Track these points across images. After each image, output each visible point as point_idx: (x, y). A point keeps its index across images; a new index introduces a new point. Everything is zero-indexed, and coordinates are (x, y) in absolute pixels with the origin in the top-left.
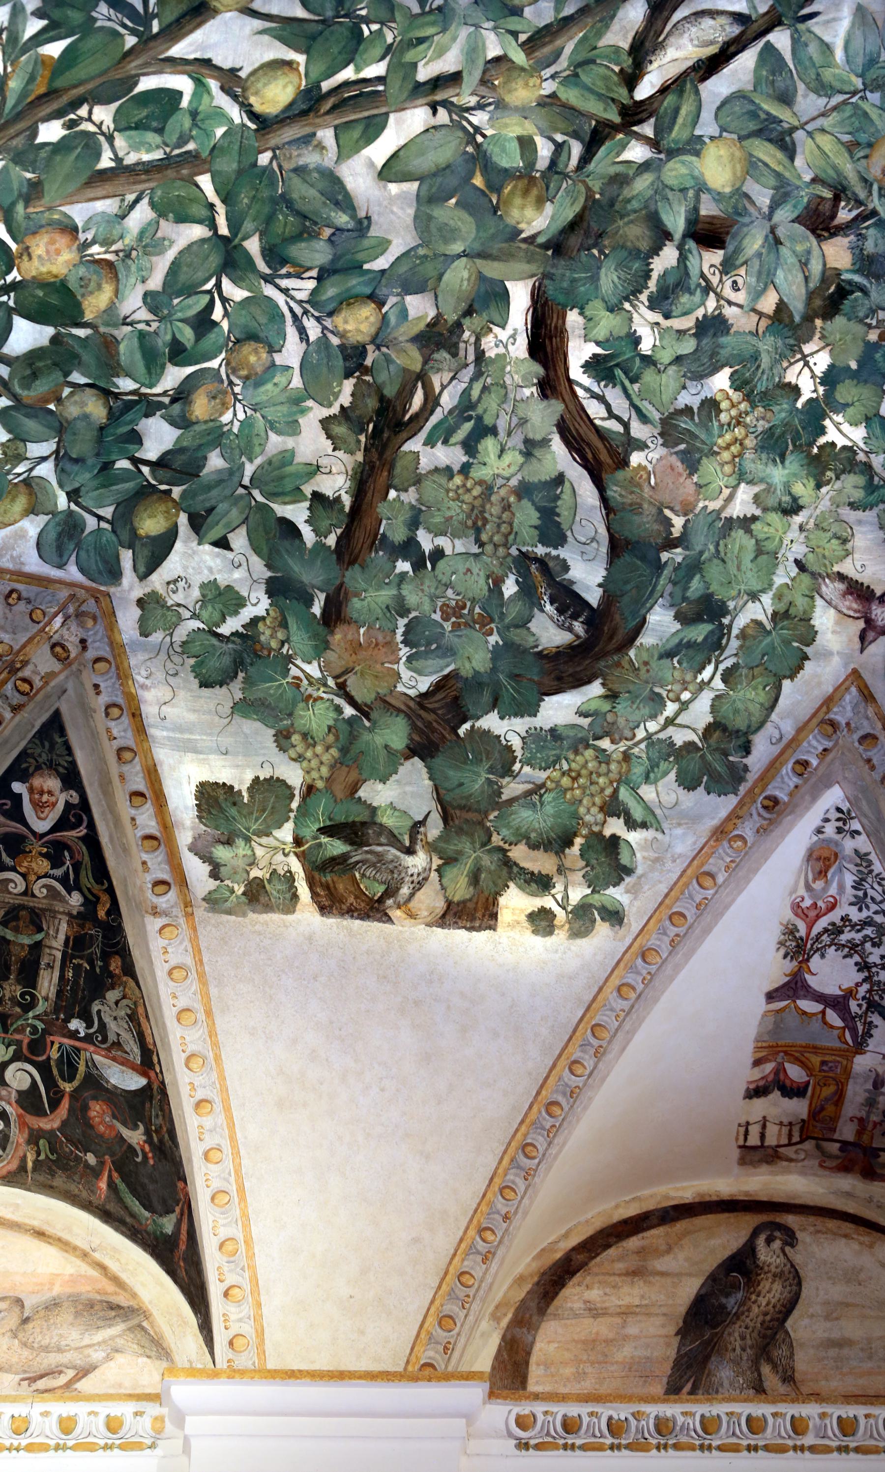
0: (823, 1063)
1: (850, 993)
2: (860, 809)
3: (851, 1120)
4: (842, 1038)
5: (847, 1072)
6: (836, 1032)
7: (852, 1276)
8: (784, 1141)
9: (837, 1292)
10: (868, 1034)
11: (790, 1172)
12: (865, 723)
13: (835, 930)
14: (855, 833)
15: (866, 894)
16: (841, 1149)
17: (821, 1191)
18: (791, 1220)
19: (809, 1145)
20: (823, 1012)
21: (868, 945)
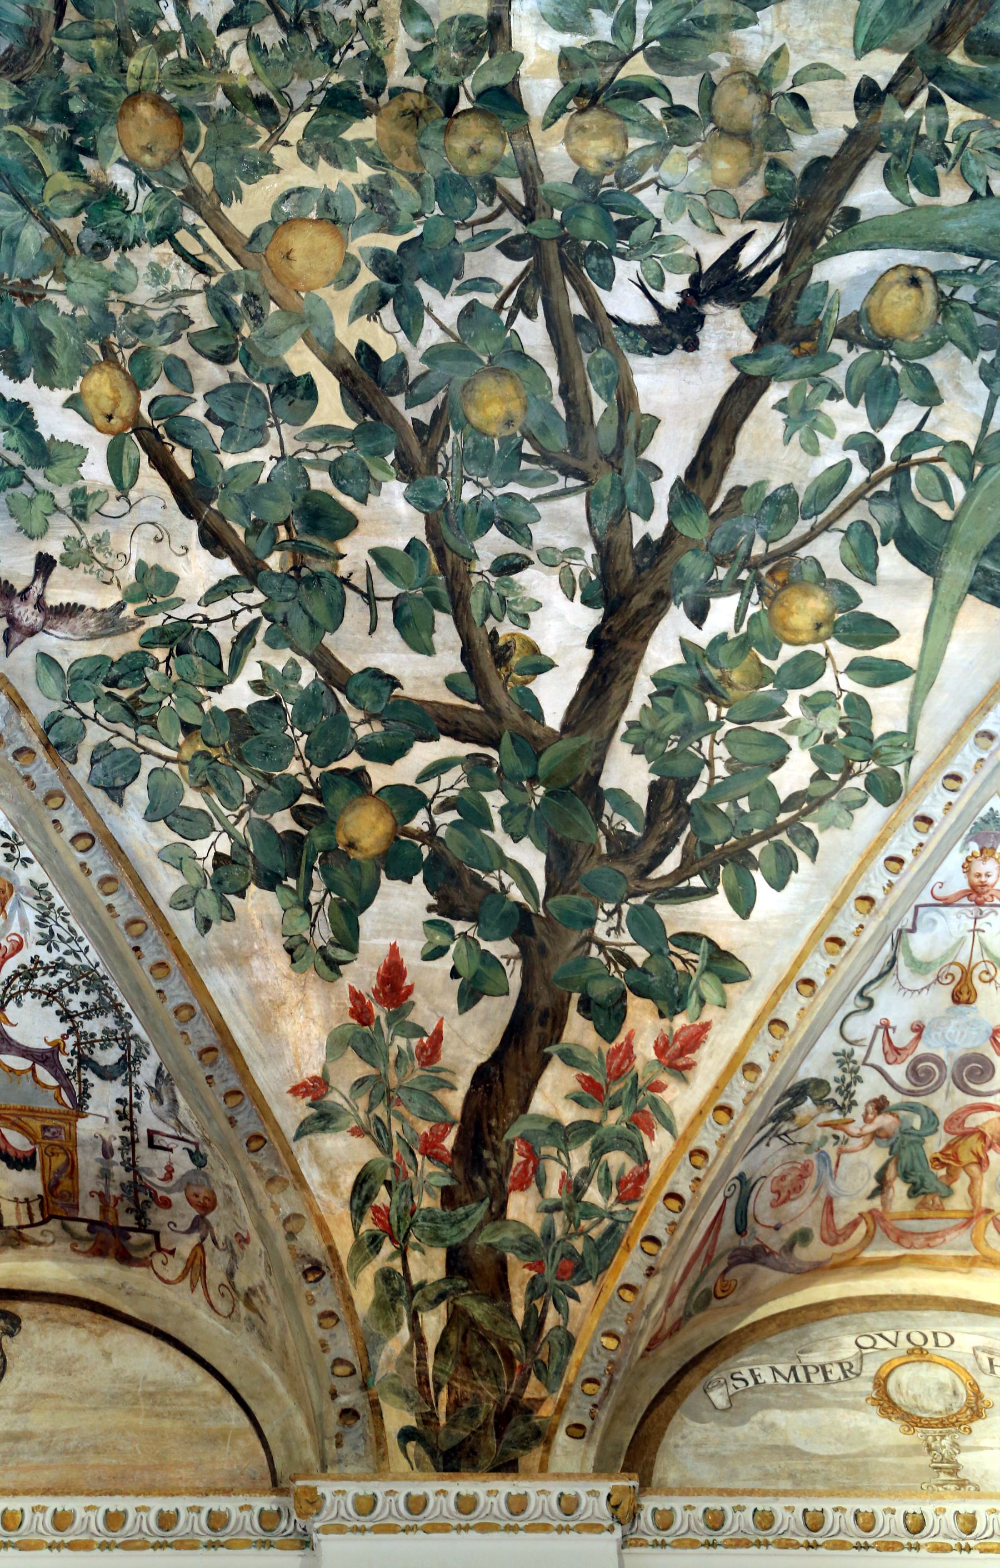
0: (45, 1128)
1: (57, 1048)
2: (26, 833)
3: (91, 1194)
4: (58, 1098)
5: (72, 1137)
6: (51, 1092)
7: (66, 1367)
8: (26, 1221)
9: (38, 1383)
10: (85, 1094)
11: (42, 1258)
12: (20, 735)
13: (27, 974)
14: (26, 861)
15: (51, 932)
16: (89, 1229)
17: (71, 1277)
18: (22, 1308)
19: (54, 1225)
20: (33, 1069)
21: (65, 991)
